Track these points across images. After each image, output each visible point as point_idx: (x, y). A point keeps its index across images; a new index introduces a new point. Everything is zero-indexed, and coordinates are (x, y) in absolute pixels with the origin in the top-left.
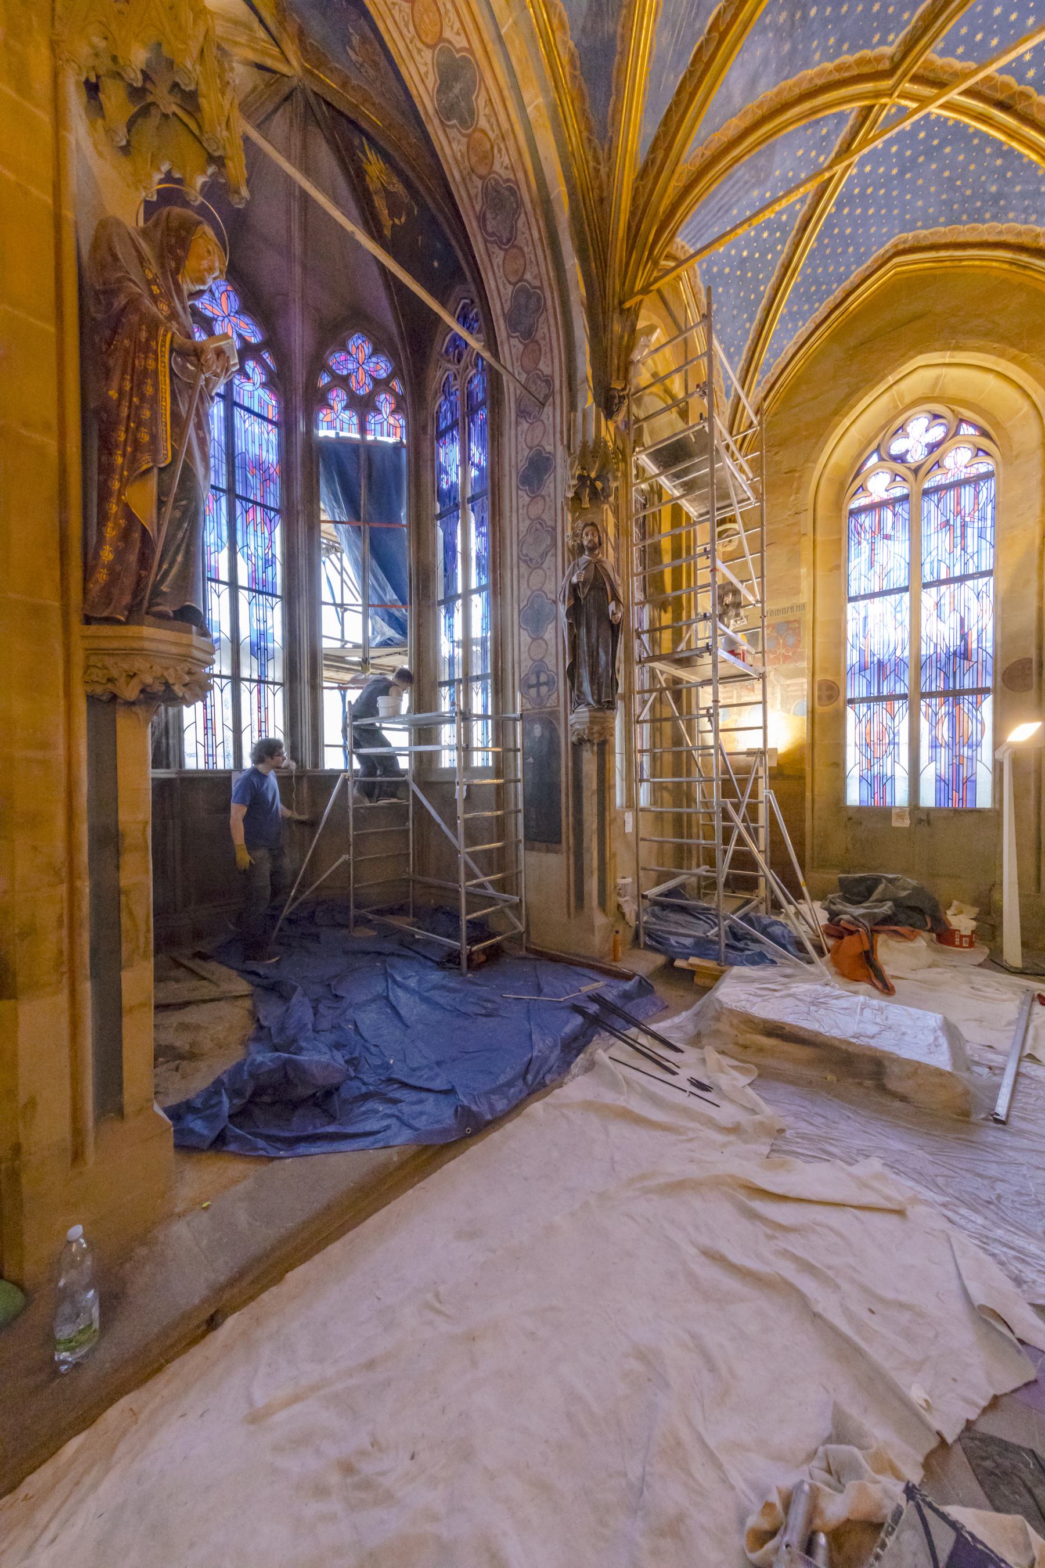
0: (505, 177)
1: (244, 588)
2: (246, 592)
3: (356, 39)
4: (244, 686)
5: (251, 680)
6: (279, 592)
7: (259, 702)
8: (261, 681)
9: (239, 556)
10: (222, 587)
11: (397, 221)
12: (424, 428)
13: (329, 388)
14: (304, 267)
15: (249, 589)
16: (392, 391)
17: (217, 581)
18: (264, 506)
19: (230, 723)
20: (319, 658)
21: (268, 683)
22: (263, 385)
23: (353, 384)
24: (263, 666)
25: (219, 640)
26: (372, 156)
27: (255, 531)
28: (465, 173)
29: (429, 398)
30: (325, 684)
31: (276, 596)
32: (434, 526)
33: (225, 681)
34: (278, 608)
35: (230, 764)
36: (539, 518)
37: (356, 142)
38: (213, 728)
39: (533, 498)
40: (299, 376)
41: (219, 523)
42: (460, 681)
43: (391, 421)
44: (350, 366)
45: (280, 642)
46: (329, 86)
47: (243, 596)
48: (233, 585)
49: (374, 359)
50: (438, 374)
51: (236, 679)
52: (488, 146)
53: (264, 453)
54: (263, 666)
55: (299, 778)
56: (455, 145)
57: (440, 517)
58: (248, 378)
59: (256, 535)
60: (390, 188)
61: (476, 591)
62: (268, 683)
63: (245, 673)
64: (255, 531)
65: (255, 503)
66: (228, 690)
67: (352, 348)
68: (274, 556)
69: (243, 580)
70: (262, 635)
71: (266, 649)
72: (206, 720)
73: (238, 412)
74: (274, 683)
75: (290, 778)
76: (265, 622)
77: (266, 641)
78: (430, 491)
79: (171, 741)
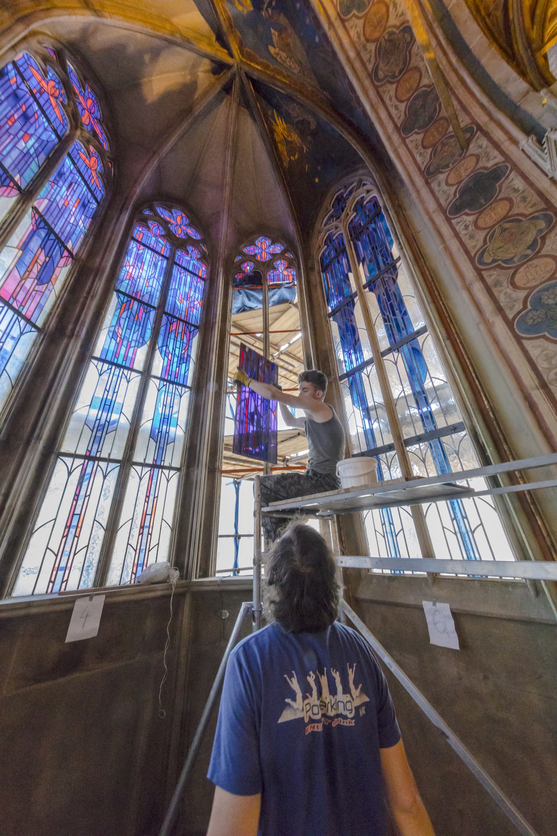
0: (398, 24)
2: (157, 381)
7: (149, 490)
8: (154, 466)
9: (157, 353)
10: (134, 374)
11: (292, 158)
12: (312, 269)
13: (243, 262)
14: (231, 193)
15: (161, 379)
16: (285, 259)
17: (131, 369)
18: (186, 323)
19: (104, 519)
20: (221, 446)
21: (164, 467)
22: (198, 259)
23: (258, 258)
24: (161, 451)
26: (279, 121)
28: (359, 48)
29: (314, 252)
30: (225, 467)
32: (328, 322)
35: (89, 582)
36: (505, 217)
37: (270, 113)
38: (79, 527)
39: (480, 213)
40: (223, 251)
42: (390, 448)
43: (285, 273)
44: (257, 251)
46: (258, 64)
48: (146, 374)
49: (272, 246)
50: (320, 237)
51: (126, 463)
52: (384, 9)
53: (192, 293)
54: (161, 451)
55: (180, 596)
56: (352, 33)
57: (333, 313)
58: (188, 254)
59: (175, 339)
60: (289, 139)
61: (389, 351)
62: (164, 467)
63: (138, 457)
65: (180, 320)
67: (257, 243)
68: (189, 356)
70: (166, 420)
71: (167, 433)
72: (72, 514)
73: (175, 268)
75: (169, 596)
76: (171, 407)
77: (169, 424)
78: (321, 299)
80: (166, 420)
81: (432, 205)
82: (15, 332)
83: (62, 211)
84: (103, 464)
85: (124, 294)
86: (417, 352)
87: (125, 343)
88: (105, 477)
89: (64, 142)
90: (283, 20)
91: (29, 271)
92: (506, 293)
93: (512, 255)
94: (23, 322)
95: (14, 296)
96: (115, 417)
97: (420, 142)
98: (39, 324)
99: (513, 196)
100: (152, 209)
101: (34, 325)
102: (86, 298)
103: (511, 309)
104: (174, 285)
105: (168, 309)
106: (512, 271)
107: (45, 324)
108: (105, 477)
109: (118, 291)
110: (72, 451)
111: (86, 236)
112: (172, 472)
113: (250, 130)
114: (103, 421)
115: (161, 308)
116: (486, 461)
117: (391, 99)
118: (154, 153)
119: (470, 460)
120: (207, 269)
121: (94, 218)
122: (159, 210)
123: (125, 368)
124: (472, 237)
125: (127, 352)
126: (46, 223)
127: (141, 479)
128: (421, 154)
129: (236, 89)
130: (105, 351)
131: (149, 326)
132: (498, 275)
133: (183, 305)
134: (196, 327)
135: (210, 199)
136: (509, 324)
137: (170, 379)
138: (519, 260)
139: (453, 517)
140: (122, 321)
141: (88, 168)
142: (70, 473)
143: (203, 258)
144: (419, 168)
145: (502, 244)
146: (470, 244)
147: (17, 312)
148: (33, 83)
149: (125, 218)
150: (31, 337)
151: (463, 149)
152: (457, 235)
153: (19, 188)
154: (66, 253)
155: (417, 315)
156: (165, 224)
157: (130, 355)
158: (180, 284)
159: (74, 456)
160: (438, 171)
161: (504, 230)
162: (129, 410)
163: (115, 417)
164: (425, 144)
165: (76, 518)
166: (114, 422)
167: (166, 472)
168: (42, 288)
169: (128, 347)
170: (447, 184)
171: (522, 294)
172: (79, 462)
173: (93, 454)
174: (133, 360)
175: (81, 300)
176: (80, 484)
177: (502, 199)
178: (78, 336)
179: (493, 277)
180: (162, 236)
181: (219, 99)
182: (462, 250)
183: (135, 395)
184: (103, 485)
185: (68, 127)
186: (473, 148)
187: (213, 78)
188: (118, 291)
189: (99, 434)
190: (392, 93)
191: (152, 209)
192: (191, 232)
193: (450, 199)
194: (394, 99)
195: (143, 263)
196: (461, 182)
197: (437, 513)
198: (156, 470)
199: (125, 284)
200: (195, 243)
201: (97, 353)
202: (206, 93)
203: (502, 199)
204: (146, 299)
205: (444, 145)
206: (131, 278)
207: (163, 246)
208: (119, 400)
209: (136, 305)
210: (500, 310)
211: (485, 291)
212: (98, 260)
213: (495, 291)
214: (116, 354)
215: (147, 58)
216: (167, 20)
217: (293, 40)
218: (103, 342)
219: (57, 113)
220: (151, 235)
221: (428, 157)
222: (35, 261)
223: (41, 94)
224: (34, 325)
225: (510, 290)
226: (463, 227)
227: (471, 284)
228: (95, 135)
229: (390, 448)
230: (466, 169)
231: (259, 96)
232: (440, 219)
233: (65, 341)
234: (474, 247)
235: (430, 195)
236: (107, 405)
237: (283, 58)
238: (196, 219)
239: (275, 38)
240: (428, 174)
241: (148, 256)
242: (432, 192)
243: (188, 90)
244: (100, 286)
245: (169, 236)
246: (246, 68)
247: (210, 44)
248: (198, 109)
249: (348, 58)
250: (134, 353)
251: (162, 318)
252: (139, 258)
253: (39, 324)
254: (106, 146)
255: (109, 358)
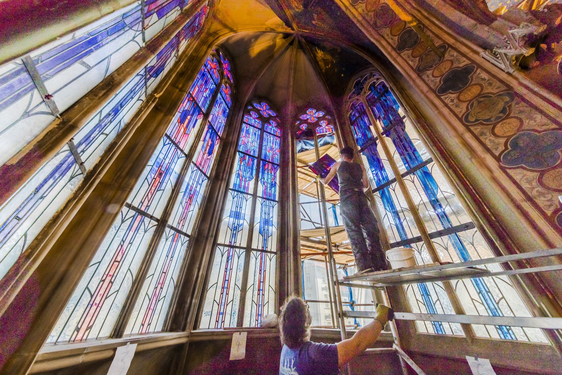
1: (259, 197)
2: (260, 199)
3: (315, 16)
4: (253, 254)
5: (257, 250)
6: (277, 199)
9: (259, 182)
10: (249, 196)
15: (262, 198)
17: (247, 194)
18: (273, 163)
22: (276, 127)
24: (265, 241)
25: (242, 225)
27: (268, 172)
31: (274, 201)
33: (242, 251)
34: (276, 206)
36: (479, 95)
39: (460, 93)
41: (252, 169)
45: (276, 226)
47: (259, 201)
48: (255, 196)
54: (265, 241)
59: (268, 174)
64: (268, 172)
65: (269, 162)
66: (243, 256)
68: (275, 183)
69: (260, 193)
70: (267, 222)
73: (265, 133)
74: (271, 252)
76: (269, 214)
79: (193, 301)
80: (267, 222)
81: (425, 89)
82: (200, 182)
83: (217, 118)
84: (237, 250)
85: (242, 152)
86: (427, 175)
87: (244, 179)
88: (239, 257)
89: (218, 86)
90: (319, 9)
91: (205, 150)
92: (490, 140)
93: (489, 117)
94: (203, 175)
95: (200, 164)
96: (241, 222)
97: (410, 55)
98: (208, 175)
99: (482, 82)
100: (252, 105)
101: (207, 176)
102: (227, 158)
103: (496, 149)
104: (265, 143)
105: (263, 157)
106: (491, 126)
107: (210, 175)
108: (239, 257)
109: (239, 151)
110: (223, 243)
111: (225, 126)
112: (272, 255)
113: (303, 59)
114: (236, 225)
115: (259, 158)
116: (498, 254)
117: (388, 35)
118: (254, 80)
119: (486, 252)
120: (281, 131)
121: (228, 117)
122: (255, 105)
123: (244, 193)
124: (457, 106)
125: (245, 184)
126: (212, 126)
127: (256, 259)
128: (412, 61)
129: (296, 43)
130: (235, 185)
131: (254, 168)
132: (482, 129)
133: (270, 154)
134: (278, 165)
135: (280, 95)
136: (497, 159)
137: (267, 198)
138: (495, 120)
139: (478, 291)
140: (242, 167)
141: (225, 94)
142: (222, 256)
143: (279, 126)
144: (412, 68)
145: (480, 110)
146: (457, 110)
147: (201, 171)
148: (209, 66)
149: (241, 114)
150: (206, 182)
151: (440, 57)
152: (446, 105)
153: (203, 114)
154: (218, 138)
155: (424, 152)
156: (258, 111)
157: (246, 185)
158: (268, 142)
159: (225, 245)
160: (425, 69)
161: (479, 102)
162: (248, 218)
163: (241, 222)
164: (413, 55)
165: (226, 282)
166: (241, 225)
167: (269, 254)
168: (209, 157)
169: (245, 181)
170: (433, 76)
171: (503, 141)
172: (226, 248)
173: (232, 244)
174: (248, 188)
175: (225, 160)
176: (227, 262)
177: (475, 85)
178: (225, 179)
179: (478, 130)
180: (256, 118)
181: (287, 49)
182: (451, 114)
183: (250, 208)
184: (238, 261)
185: (219, 80)
186: (447, 56)
187: (284, 41)
188: (239, 151)
189: (235, 232)
190: (389, 32)
191: (252, 105)
192: (271, 113)
193: (437, 85)
194: (390, 35)
195: (249, 134)
196: (443, 75)
197: (465, 289)
198: (264, 253)
199: (241, 147)
200: (273, 118)
201: (231, 186)
202: (280, 47)
203: (475, 85)
204: (252, 154)
205: (426, 55)
206: (244, 143)
207: (258, 123)
208: (243, 212)
209: (247, 156)
210: (488, 150)
211: (474, 138)
212: (231, 138)
213: (482, 138)
214: (240, 186)
215: (253, 40)
216: (264, 24)
217: (325, 16)
218: (234, 179)
219: (216, 75)
220: (252, 119)
221: (417, 62)
222: (208, 145)
223: (211, 69)
224: (207, 176)
225: (492, 138)
226: (450, 100)
227: (462, 134)
228: (228, 78)
229: (418, 239)
230: (445, 68)
231: (308, 44)
232: (432, 96)
233: (219, 183)
234: (461, 112)
235: (422, 82)
236: (237, 215)
237: (321, 24)
238: (273, 106)
239: (315, 18)
240: (419, 71)
241: (251, 130)
242: (424, 81)
243: (271, 49)
244: (232, 151)
245: (261, 117)
246: (301, 33)
247: (283, 28)
248: (276, 55)
249: (358, 21)
250: (248, 185)
251: (261, 162)
252: (247, 132)
253: (208, 175)
254: (232, 81)
255: (237, 189)
